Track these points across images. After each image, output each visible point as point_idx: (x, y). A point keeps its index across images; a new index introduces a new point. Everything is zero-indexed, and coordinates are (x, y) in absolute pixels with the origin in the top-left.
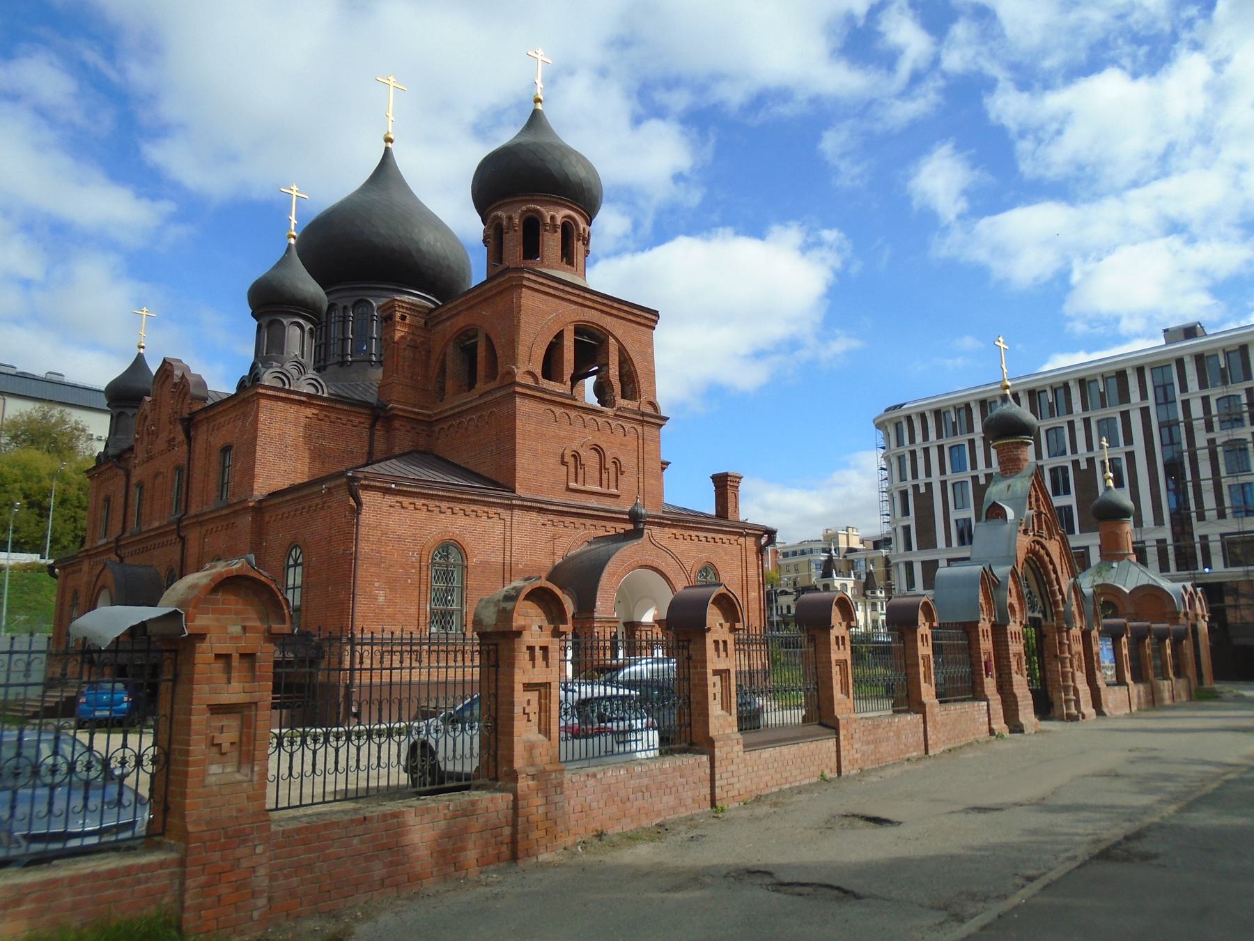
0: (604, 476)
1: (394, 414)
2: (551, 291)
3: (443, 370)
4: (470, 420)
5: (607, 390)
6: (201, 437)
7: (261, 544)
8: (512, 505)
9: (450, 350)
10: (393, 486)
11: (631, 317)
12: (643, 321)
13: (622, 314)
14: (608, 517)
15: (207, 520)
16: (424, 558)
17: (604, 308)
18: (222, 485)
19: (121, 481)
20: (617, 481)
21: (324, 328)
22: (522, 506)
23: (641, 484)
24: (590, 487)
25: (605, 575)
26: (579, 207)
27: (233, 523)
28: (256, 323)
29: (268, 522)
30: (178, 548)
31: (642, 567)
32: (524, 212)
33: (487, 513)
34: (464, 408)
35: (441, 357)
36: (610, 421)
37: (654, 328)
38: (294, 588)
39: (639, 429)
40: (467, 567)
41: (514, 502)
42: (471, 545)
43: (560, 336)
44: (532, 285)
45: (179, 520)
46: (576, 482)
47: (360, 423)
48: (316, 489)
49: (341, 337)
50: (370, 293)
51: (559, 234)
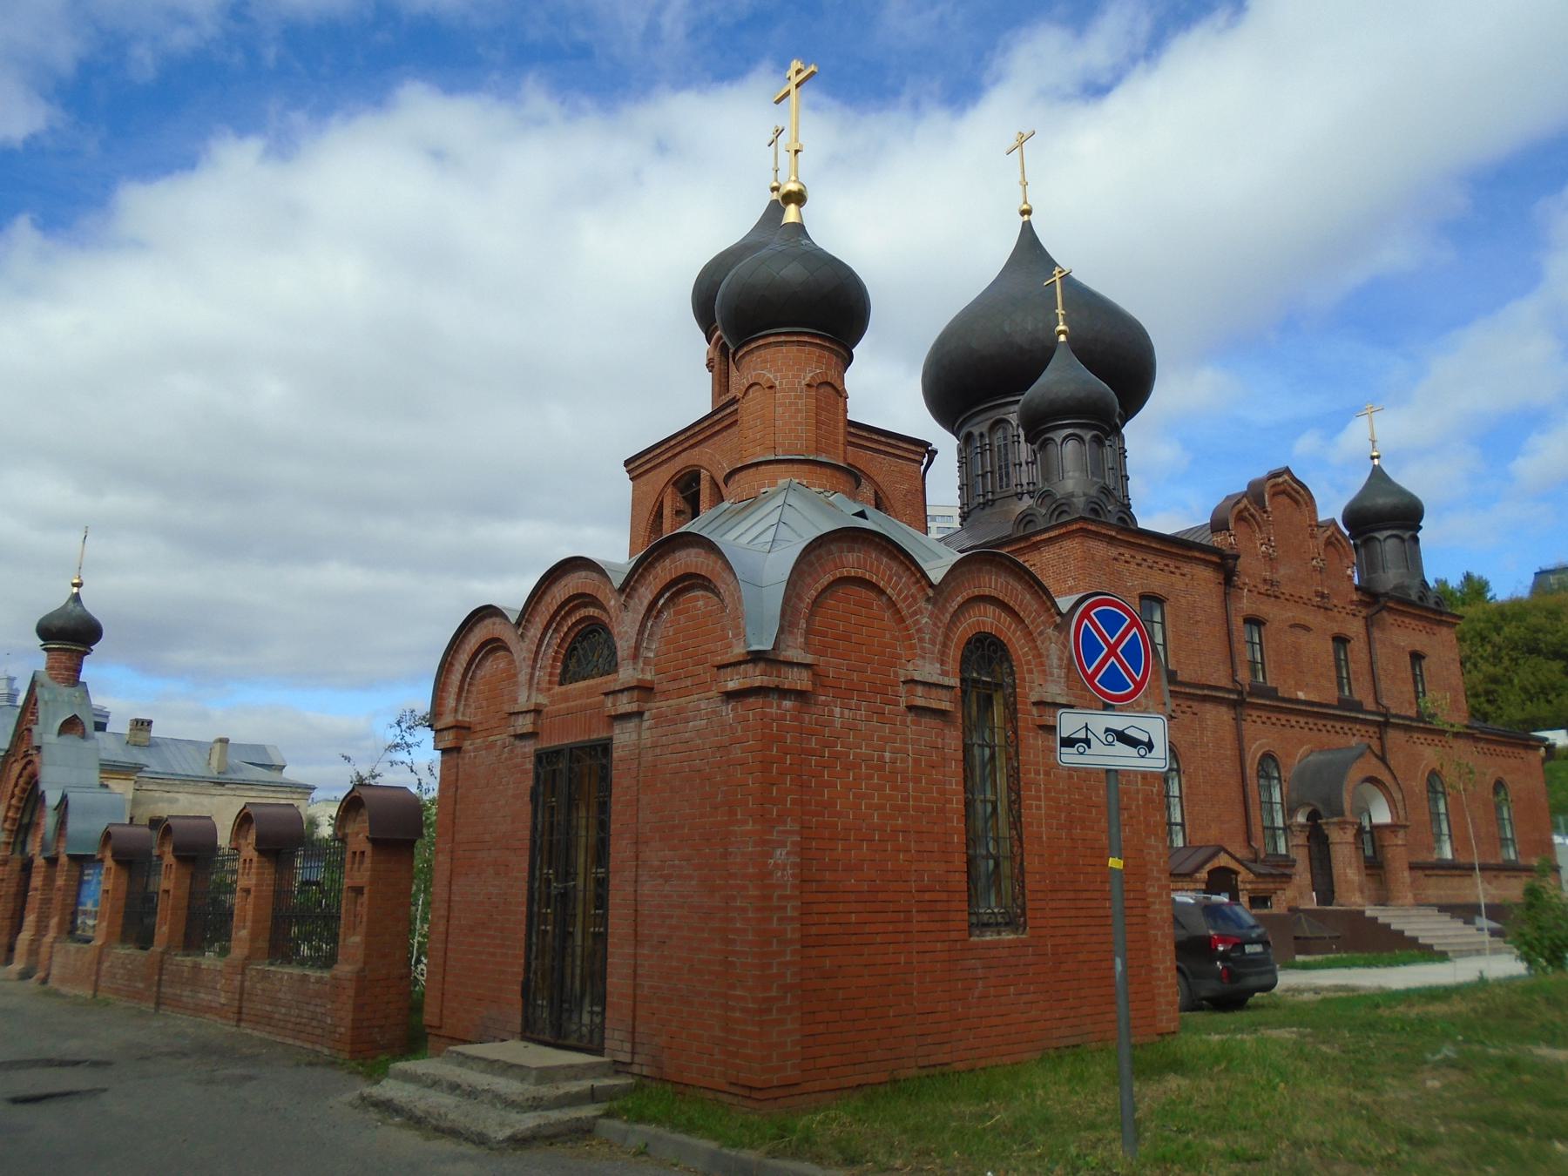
2: (649, 466)
11: (717, 428)
13: (708, 433)
17: (692, 442)
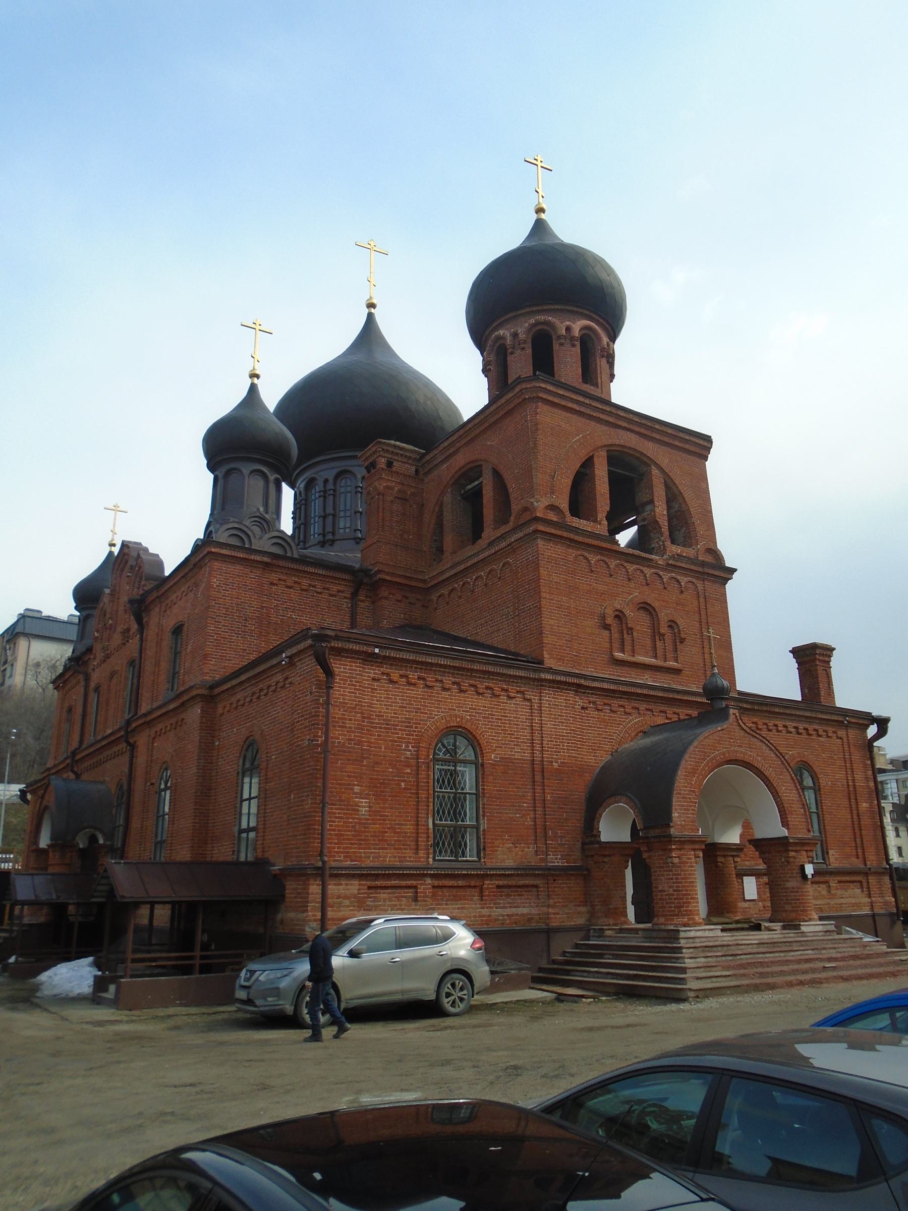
0: (659, 644)
1: (380, 579)
2: (575, 407)
3: (440, 525)
4: (476, 579)
5: (652, 535)
6: (154, 620)
7: (213, 743)
8: (542, 680)
9: (448, 499)
10: (377, 651)
11: (677, 443)
12: (692, 448)
13: (666, 439)
14: (670, 699)
15: (155, 718)
16: (423, 752)
18: (174, 674)
19: (81, 689)
20: (676, 650)
21: (303, 507)
22: (553, 681)
23: (707, 656)
24: (641, 659)
25: (681, 773)
26: (600, 316)
27: (183, 719)
28: (212, 476)
29: (222, 714)
30: (126, 758)
31: (729, 762)
32: (534, 325)
33: (507, 690)
34: (469, 564)
35: (437, 509)
36: (661, 573)
37: (706, 458)
38: (250, 799)
39: (699, 585)
40: (482, 765)
41: (543, 676)
42: (486, 733)
43: (588, 464)
45: (128, 722)
46: (623, 651)
47: (339, 591)
48: (275, 661)
49: (323, 514)
50: (355, 462)
51: (578, 349)
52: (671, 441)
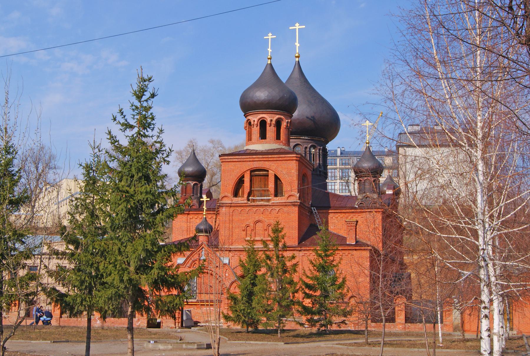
11: (280, 159)
13: (275, 159)
17: (264, 159)
44: (227, 160)
51: (259, 127)
52: (278, 159)
